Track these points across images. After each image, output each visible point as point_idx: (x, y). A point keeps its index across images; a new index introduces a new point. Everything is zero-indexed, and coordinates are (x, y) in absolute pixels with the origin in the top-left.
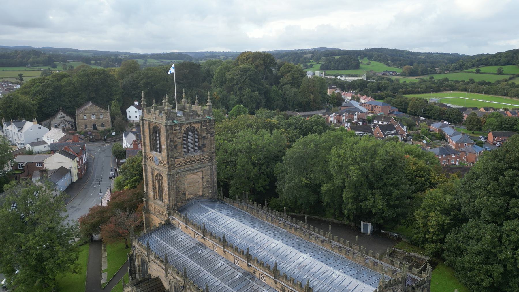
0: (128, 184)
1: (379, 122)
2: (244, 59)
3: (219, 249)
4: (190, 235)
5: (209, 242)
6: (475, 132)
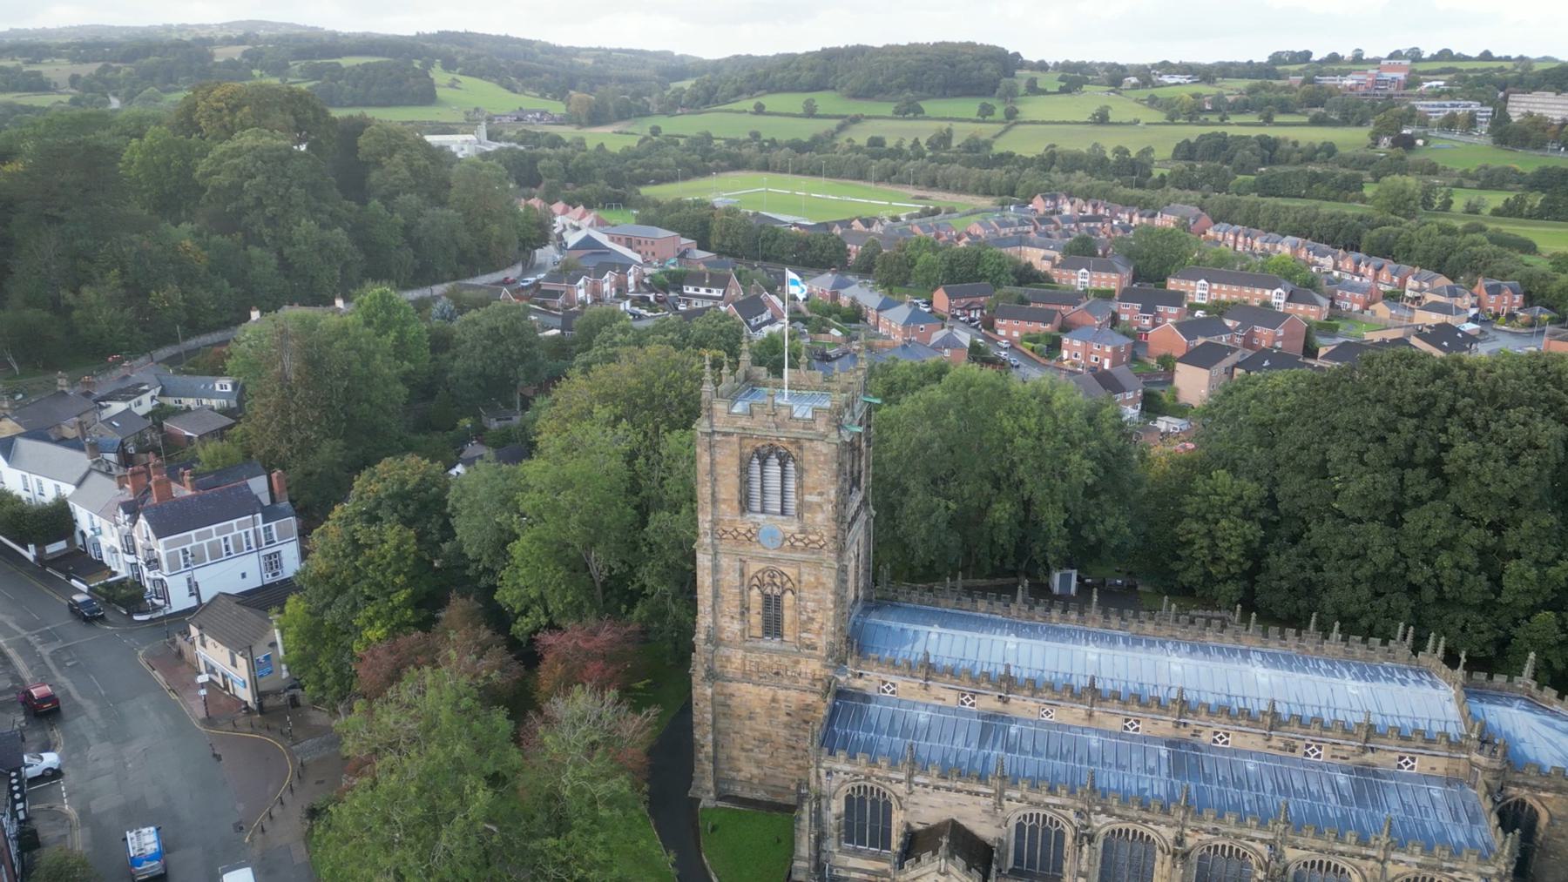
0: (371, 622)
1: (697, 290)
2: (219, 110)
3: (1071, 714)
4: (940, 703)
5: (1022, 706)
6: (895, 289)
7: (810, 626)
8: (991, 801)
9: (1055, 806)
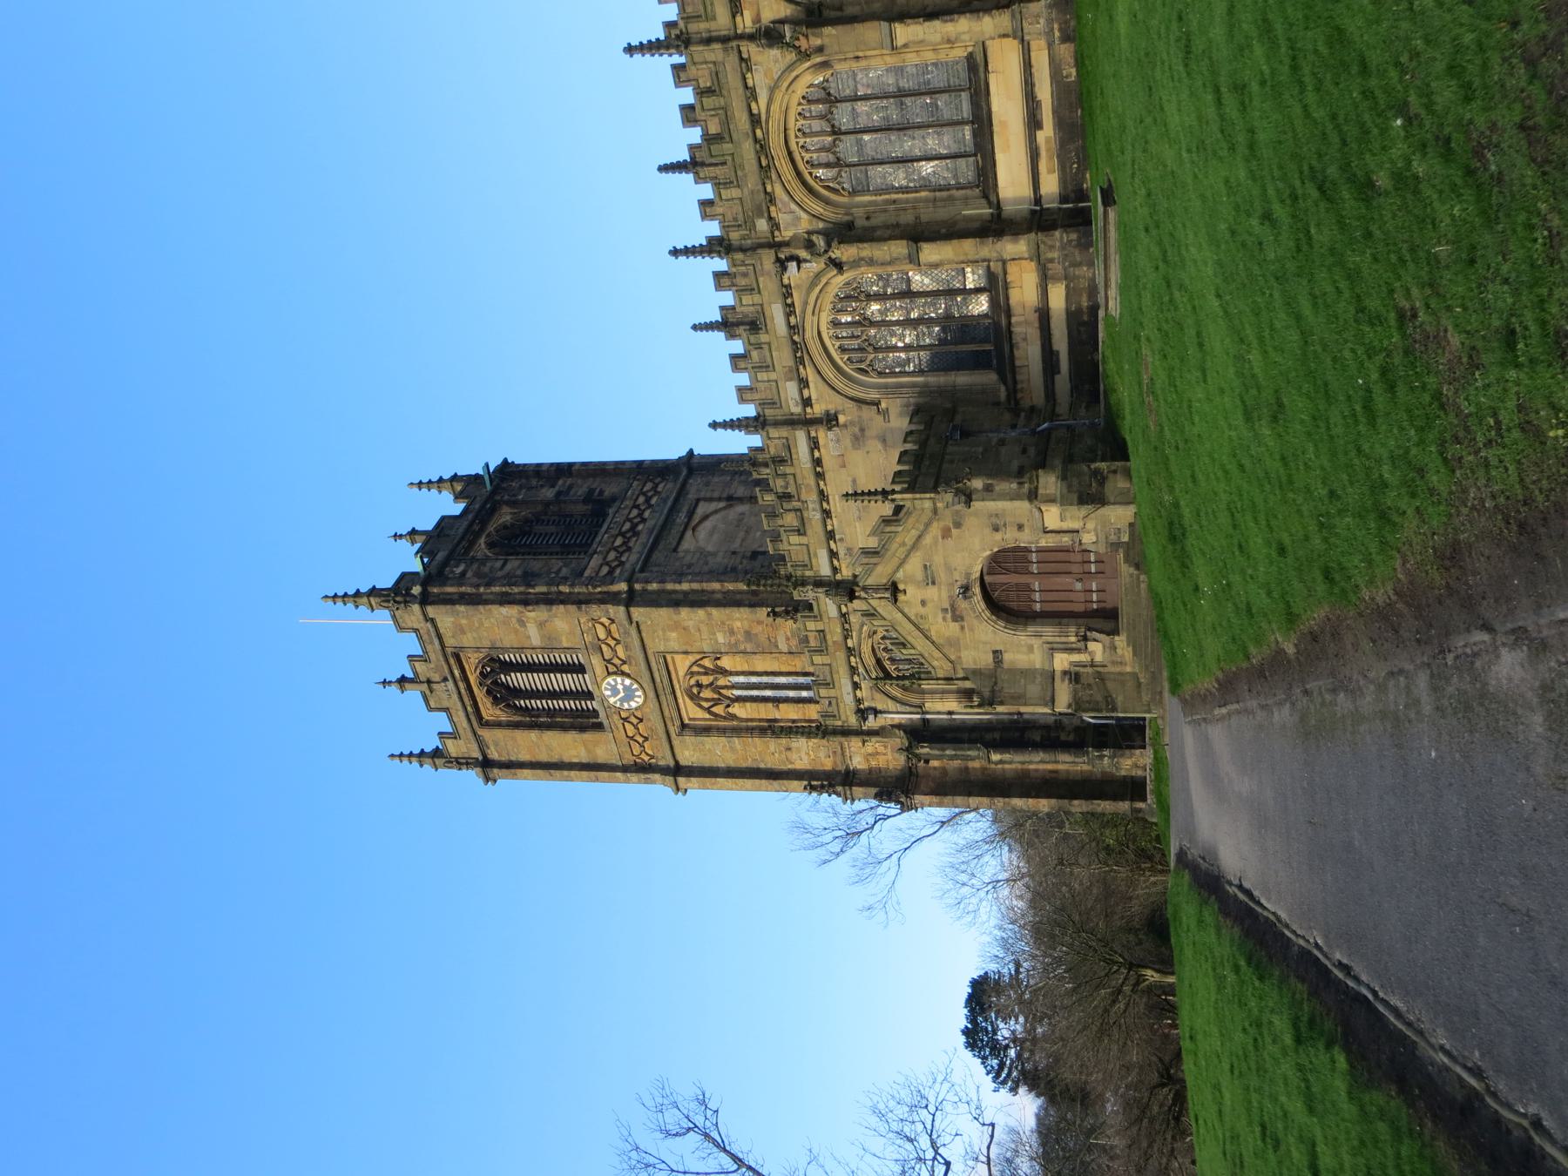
7: (763, 639)
8: (823, 435)
9: (790, 310)
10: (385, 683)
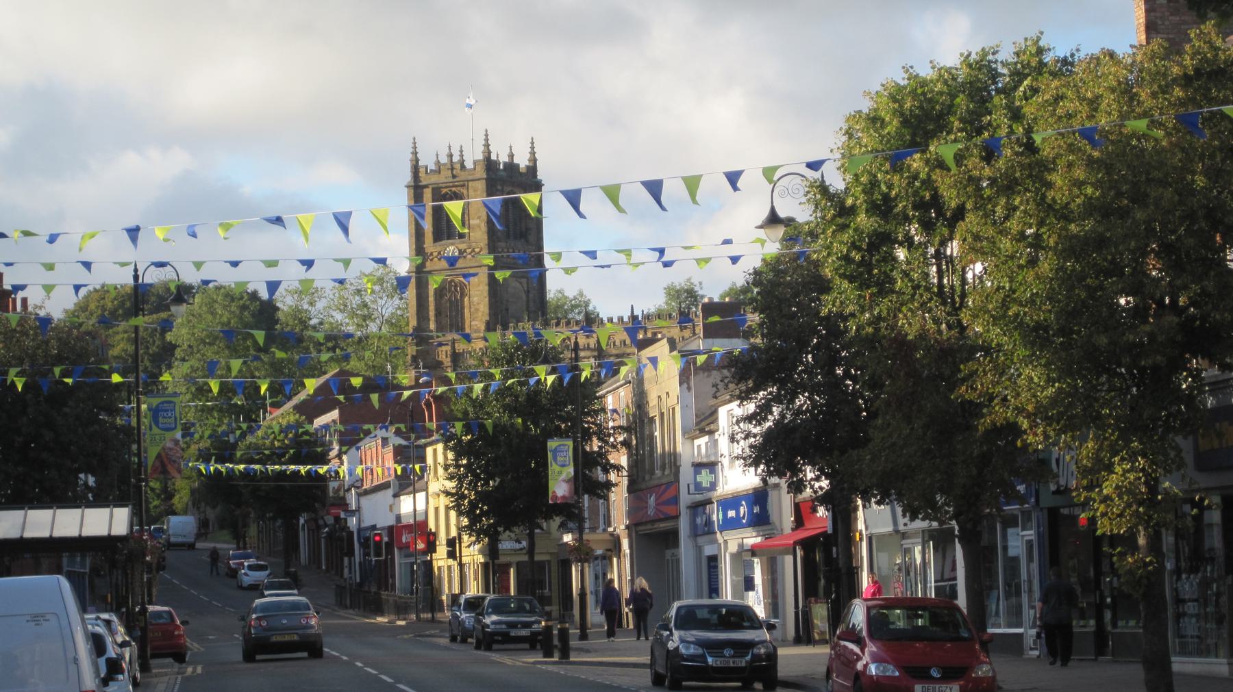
10: (450, 147)
